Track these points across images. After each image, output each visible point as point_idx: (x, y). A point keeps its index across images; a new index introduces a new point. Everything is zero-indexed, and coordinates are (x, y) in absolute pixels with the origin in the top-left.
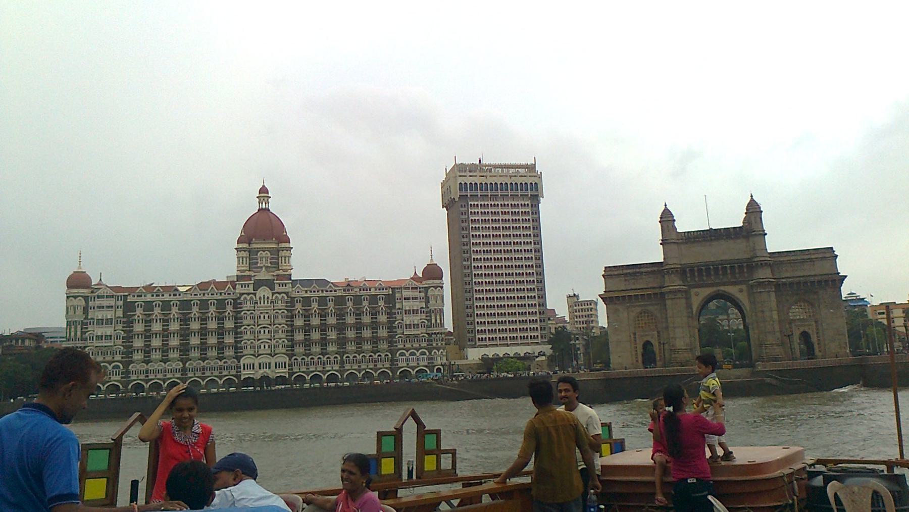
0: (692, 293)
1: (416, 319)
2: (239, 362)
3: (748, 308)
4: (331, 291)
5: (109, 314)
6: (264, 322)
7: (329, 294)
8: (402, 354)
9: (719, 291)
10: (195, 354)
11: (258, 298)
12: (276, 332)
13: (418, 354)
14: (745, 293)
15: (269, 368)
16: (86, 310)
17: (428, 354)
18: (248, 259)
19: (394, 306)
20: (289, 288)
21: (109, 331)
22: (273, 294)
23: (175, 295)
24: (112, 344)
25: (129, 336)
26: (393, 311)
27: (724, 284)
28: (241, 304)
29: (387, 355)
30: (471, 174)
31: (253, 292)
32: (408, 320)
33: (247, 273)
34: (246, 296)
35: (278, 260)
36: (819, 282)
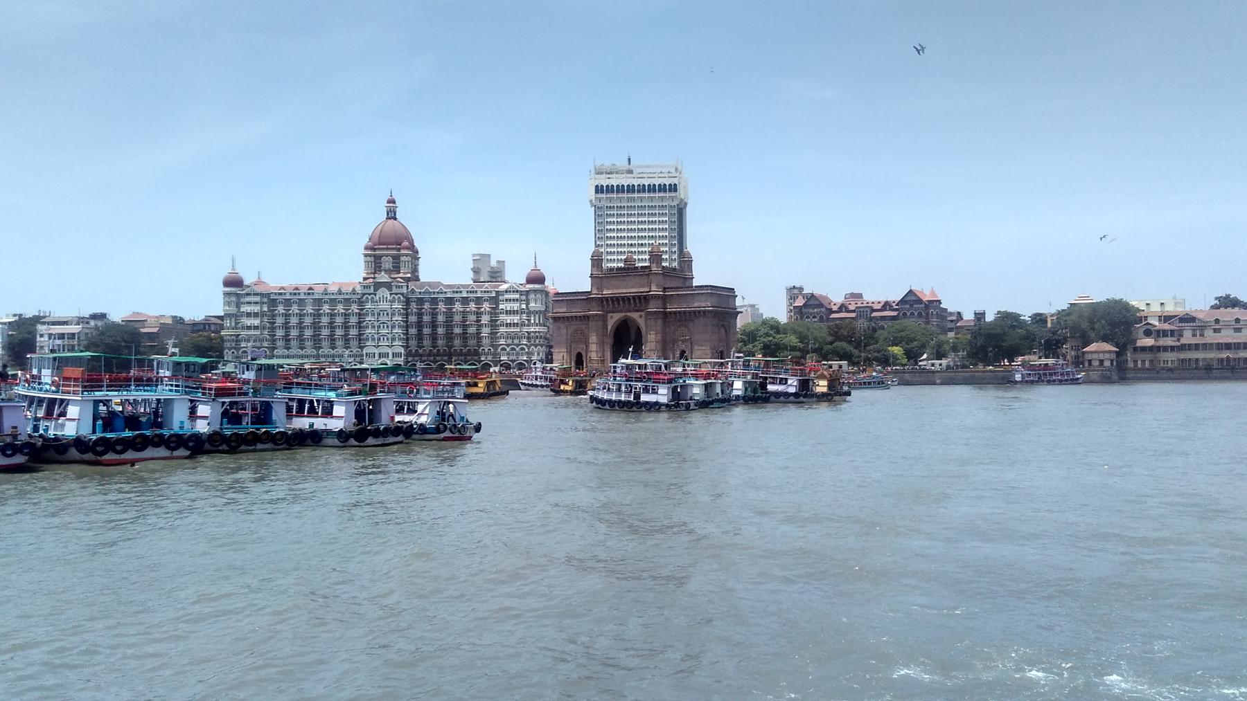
0: (609, 317)
1: (516, 319)
2: (362, 351)
3: (644, 330)
4: (442, 293)
5: (256, 309)
6: (383, 319)
7: (440, 296)
8: (503, 349)
9: (626, 316)
10: (325, 344)
11: (377, 298)
12: (393, 327)
13: (518, 349)
14: (643, 319)
15: (388, 357)
16: (238, 305)
17: (527, 350)
18: (373, 263)
19: (497, 307)
20: (404, 290)
21: (256, 322)
22: (391, 294)
23: (309, 294)
24: (259, 333)
25: (273, 329)
26: (497, 311)
27: (630, 311)
28: (362, 302)
29: (490, 349)
30: (608, 176)
31: (372, 292)
32: (509, 319)
33: (372, 276)
34: (367, 296)
35: (399, 264)
36: (694, 312)
